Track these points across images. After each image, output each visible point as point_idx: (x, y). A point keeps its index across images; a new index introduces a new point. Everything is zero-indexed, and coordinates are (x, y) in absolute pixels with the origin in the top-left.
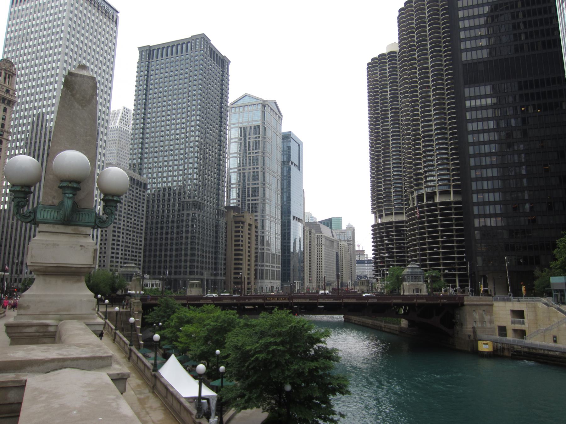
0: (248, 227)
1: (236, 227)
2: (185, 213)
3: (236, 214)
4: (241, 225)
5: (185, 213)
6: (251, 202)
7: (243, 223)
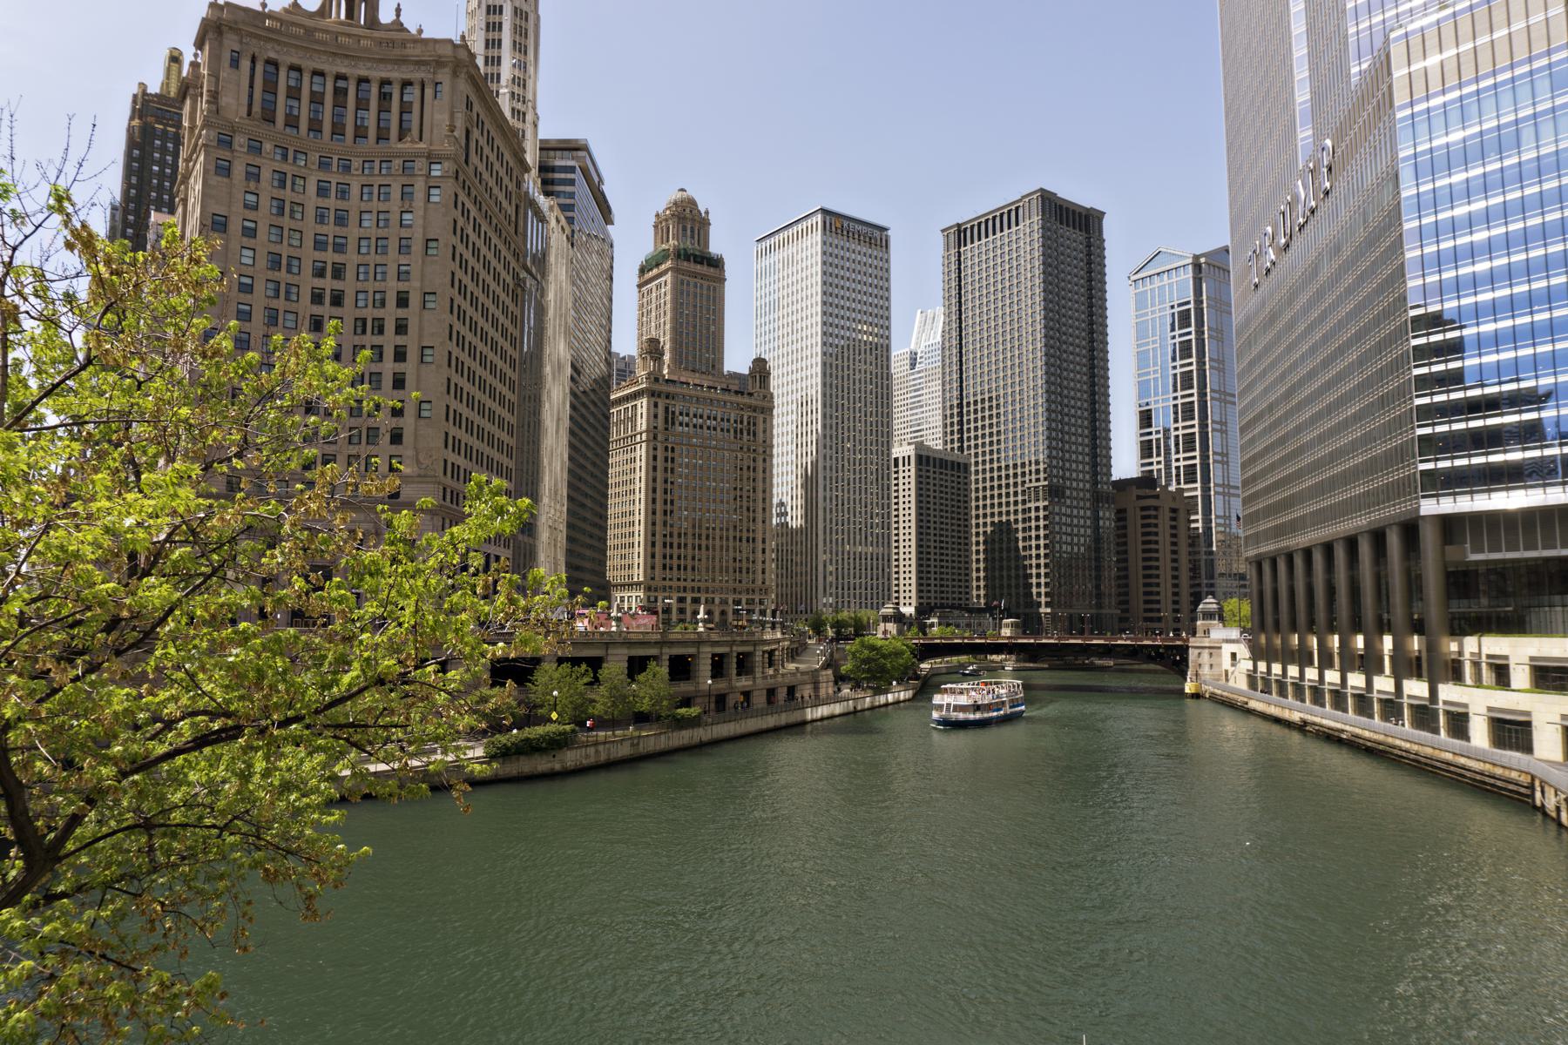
0: (1168, 515)
1: (1144, 517)
2: (1032, 505)
3: (1141, 492)
4: (1153, 513)
5: (1032, 505)
6: (1182, 463)
7: (1156, 508)
